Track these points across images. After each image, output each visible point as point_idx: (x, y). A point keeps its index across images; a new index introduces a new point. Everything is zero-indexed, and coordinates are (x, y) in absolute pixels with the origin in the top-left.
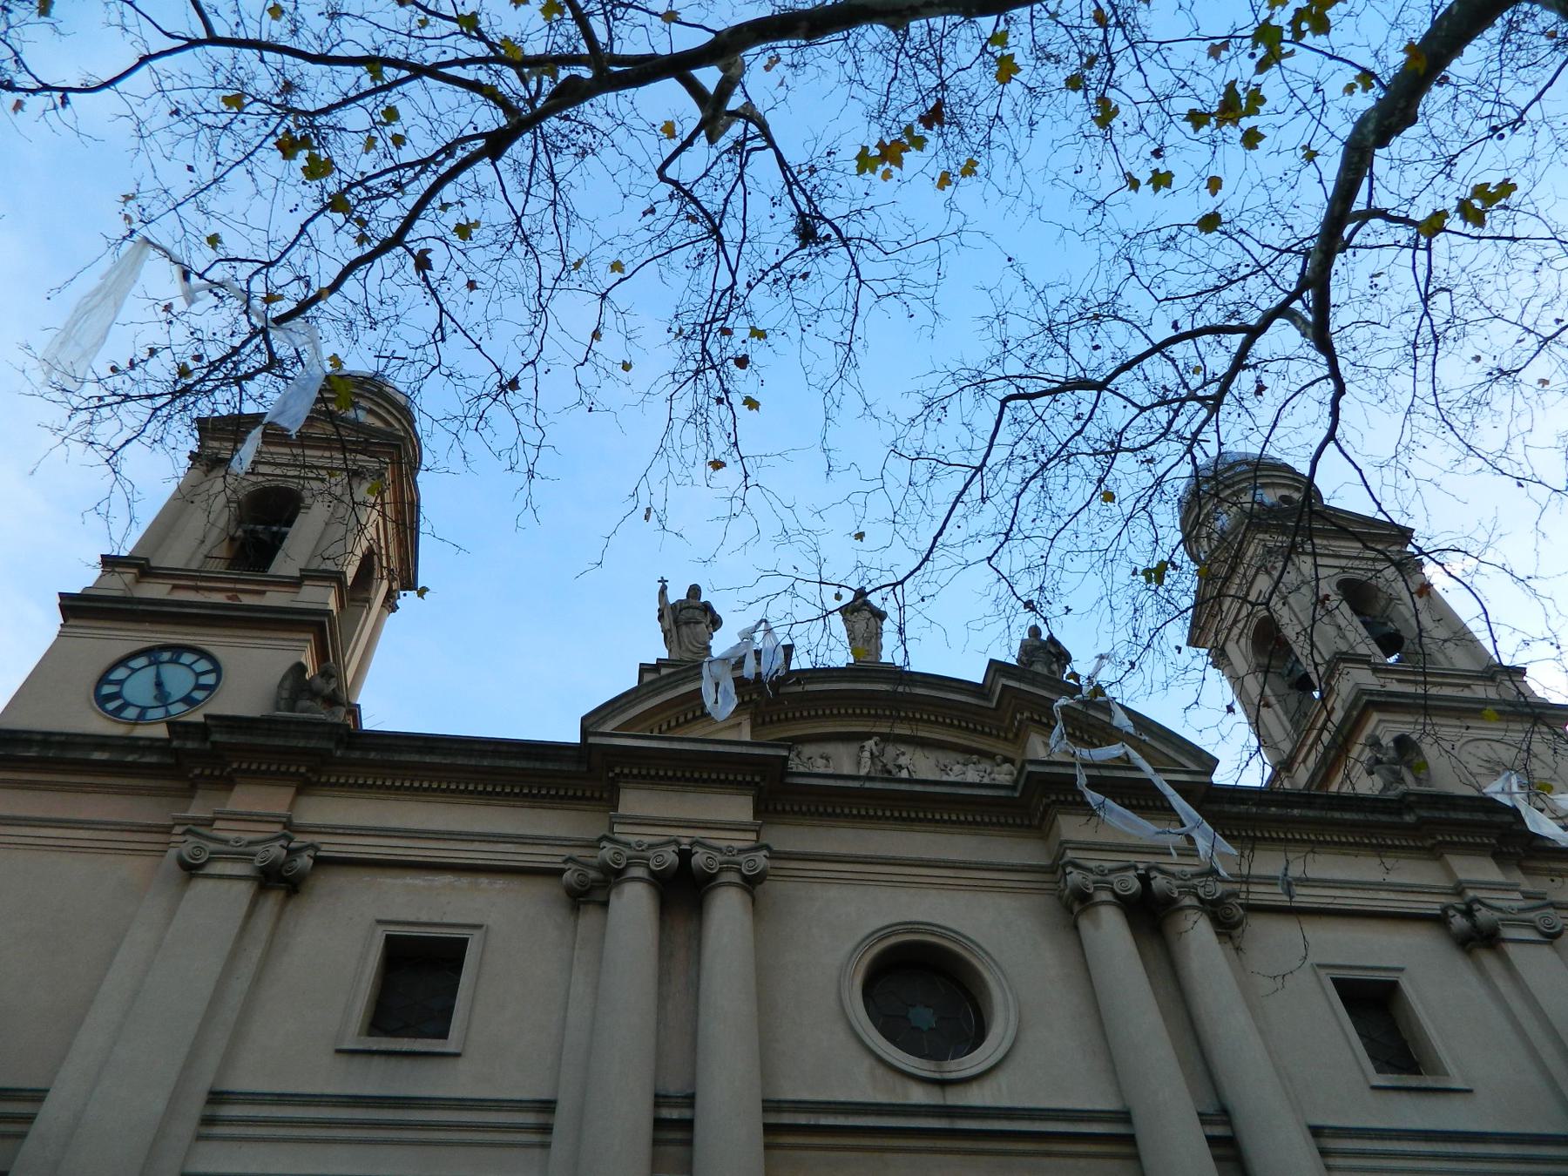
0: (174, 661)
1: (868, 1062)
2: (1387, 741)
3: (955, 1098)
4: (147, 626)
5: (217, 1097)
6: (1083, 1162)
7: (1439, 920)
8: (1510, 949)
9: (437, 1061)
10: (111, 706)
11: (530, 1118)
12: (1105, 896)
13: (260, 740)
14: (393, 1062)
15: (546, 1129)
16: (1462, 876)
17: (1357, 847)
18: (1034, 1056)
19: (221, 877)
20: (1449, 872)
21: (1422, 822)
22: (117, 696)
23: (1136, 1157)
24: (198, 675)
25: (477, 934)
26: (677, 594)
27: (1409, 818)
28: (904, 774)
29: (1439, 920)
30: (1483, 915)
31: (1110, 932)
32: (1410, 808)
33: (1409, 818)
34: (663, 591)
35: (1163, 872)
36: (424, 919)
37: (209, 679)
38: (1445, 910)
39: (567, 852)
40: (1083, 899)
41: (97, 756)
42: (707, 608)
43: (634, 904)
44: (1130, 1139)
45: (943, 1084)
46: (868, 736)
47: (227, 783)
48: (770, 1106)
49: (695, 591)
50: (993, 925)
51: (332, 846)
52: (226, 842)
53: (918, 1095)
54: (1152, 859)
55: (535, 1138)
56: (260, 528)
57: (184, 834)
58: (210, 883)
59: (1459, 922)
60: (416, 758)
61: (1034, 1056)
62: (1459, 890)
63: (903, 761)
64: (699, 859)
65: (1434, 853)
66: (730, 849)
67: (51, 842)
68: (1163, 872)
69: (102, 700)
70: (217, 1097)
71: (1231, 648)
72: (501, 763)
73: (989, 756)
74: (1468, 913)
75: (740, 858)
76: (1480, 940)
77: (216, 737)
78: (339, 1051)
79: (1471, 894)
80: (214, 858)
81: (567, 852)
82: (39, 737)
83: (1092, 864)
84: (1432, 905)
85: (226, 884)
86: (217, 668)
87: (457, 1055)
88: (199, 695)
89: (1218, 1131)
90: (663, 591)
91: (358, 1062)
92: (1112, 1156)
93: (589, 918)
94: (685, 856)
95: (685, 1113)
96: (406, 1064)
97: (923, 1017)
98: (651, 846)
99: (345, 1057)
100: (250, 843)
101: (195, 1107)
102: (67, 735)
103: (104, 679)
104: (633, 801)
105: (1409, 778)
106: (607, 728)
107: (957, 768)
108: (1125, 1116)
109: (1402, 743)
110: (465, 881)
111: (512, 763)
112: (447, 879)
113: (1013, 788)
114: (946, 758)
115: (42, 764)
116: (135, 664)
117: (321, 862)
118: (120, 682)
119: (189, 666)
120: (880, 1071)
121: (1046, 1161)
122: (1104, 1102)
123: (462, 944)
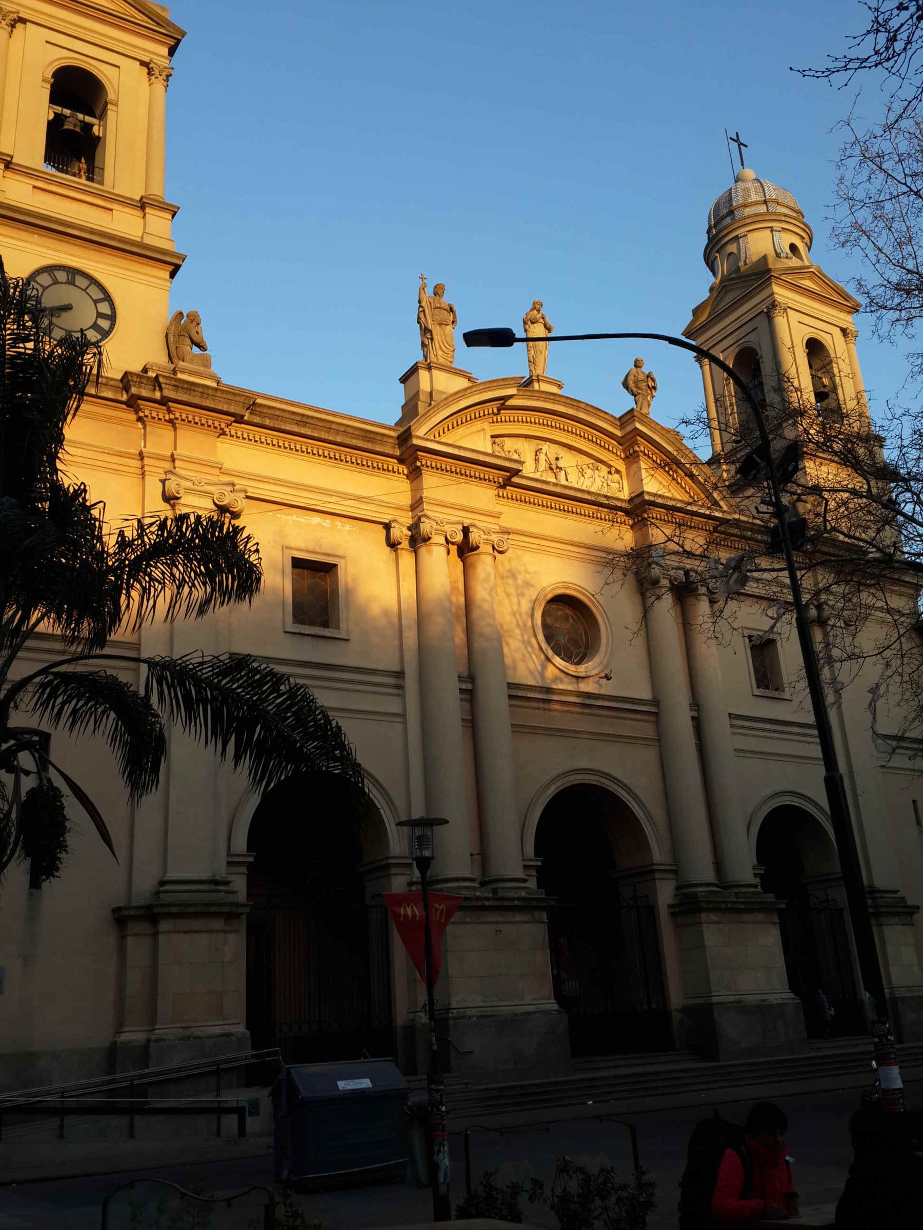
0: (71, 283)
6: (634, 723)
11: (391, 681)
14: (315, 641)
15: (401, 687)
24: (96, 302)
25: (342, 561)
37: (104, 308)
55: (395, 691)
56: (67, 112)
64: (474, 537)
78: (285, 632)
86: (108, 298)
87: (348, 640)
88: (104, 324)
89: (695, 714)
91: (297, 637)
94: (466, 531)
95: (470, 687)
96: (322, 643)
107: (589, 472)
108: (656, 702)
119: (85, 290)
122: (646, 695)
123: (335, 566)
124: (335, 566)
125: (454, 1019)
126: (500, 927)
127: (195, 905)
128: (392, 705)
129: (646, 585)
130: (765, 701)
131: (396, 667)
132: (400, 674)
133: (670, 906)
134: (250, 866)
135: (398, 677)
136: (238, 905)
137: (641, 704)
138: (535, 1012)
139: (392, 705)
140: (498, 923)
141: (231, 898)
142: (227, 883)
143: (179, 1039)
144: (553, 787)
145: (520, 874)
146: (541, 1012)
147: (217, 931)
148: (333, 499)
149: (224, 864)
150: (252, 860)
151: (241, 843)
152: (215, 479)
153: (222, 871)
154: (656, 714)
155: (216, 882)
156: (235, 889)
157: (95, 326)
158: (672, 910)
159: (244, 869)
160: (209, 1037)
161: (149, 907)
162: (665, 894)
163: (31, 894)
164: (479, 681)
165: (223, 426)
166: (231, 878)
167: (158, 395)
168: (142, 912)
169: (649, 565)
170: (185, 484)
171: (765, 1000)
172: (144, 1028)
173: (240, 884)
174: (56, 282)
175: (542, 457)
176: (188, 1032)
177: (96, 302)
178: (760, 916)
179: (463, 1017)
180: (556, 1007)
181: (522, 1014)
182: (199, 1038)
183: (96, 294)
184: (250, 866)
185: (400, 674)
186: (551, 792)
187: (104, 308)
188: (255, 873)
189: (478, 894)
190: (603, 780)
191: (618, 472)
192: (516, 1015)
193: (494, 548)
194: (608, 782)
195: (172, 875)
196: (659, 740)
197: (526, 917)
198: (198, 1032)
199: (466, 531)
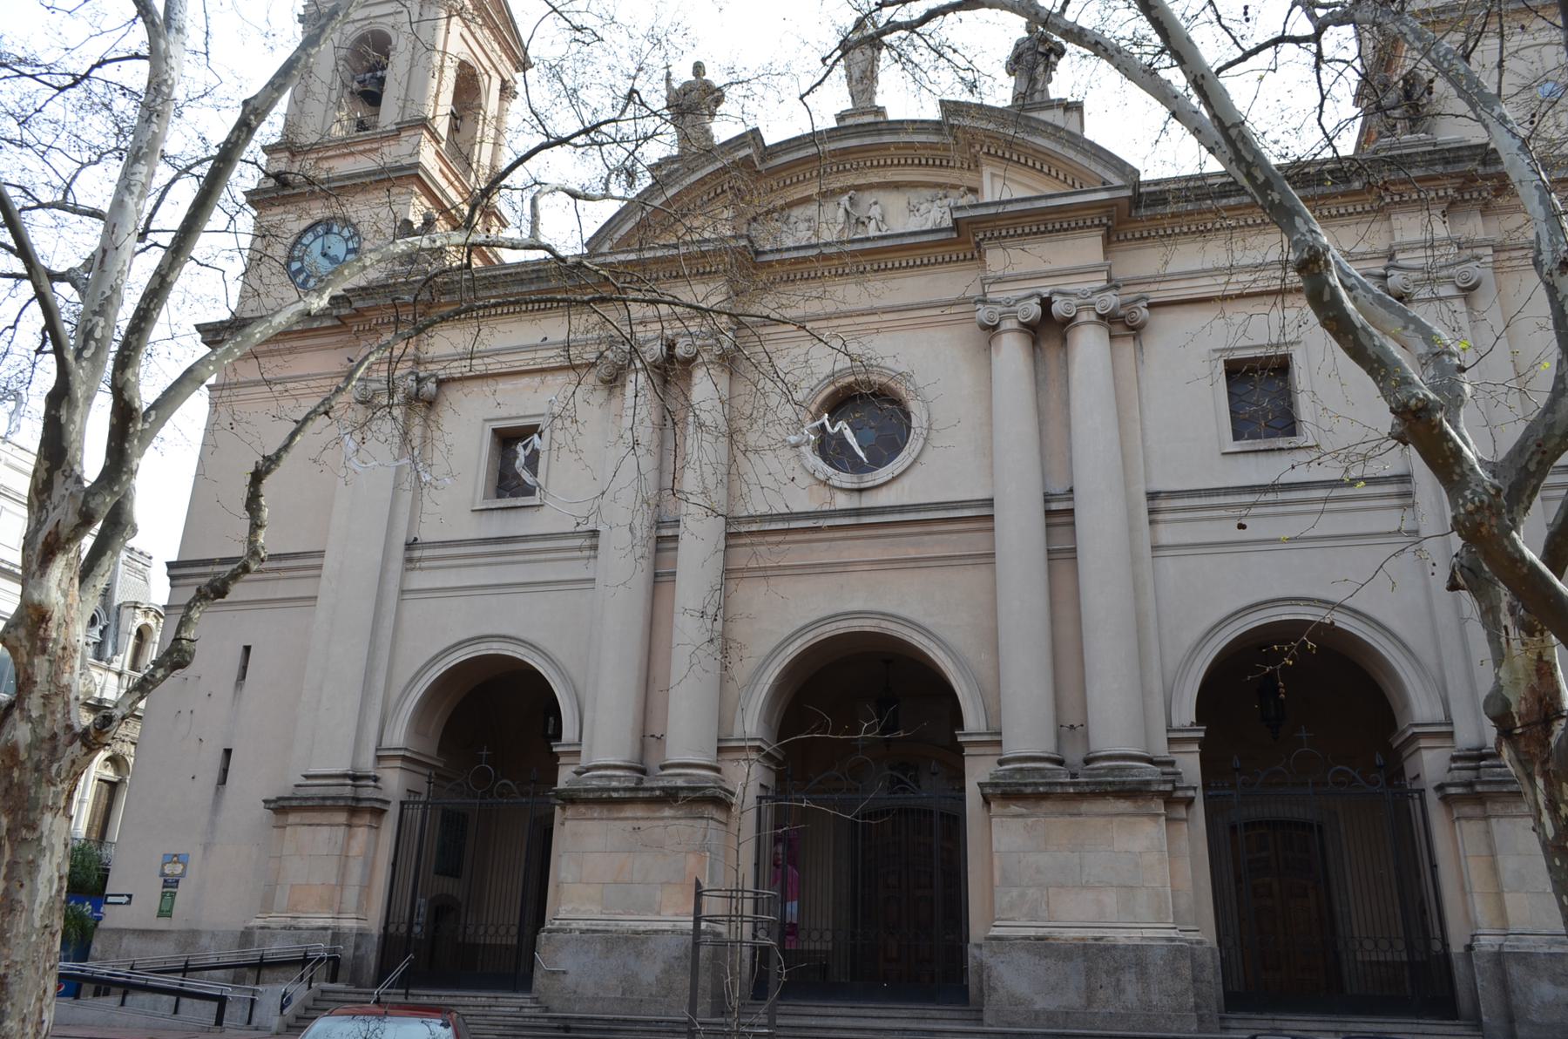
3: (868, 501)
5: (411, 545)
6: (955, 537)
22: (300, 271)
35: (1064, 294)
53: (842, 501)
55: (586, 553)
68: (1064, 294)
116: (305, 241)
117: (440, 383)
121: (927, 538)
125: (550, 931)
126: (641, 824)
127: (312, 798)
128: (577, 570)
130: (1262, 458)
137: (962, 508)
171: (1101, 938)
176: (293, 922)
179: (563, 931)
181: (645, 932)
190: (884, 624)
194: (892, 626)
198: (302, 923)
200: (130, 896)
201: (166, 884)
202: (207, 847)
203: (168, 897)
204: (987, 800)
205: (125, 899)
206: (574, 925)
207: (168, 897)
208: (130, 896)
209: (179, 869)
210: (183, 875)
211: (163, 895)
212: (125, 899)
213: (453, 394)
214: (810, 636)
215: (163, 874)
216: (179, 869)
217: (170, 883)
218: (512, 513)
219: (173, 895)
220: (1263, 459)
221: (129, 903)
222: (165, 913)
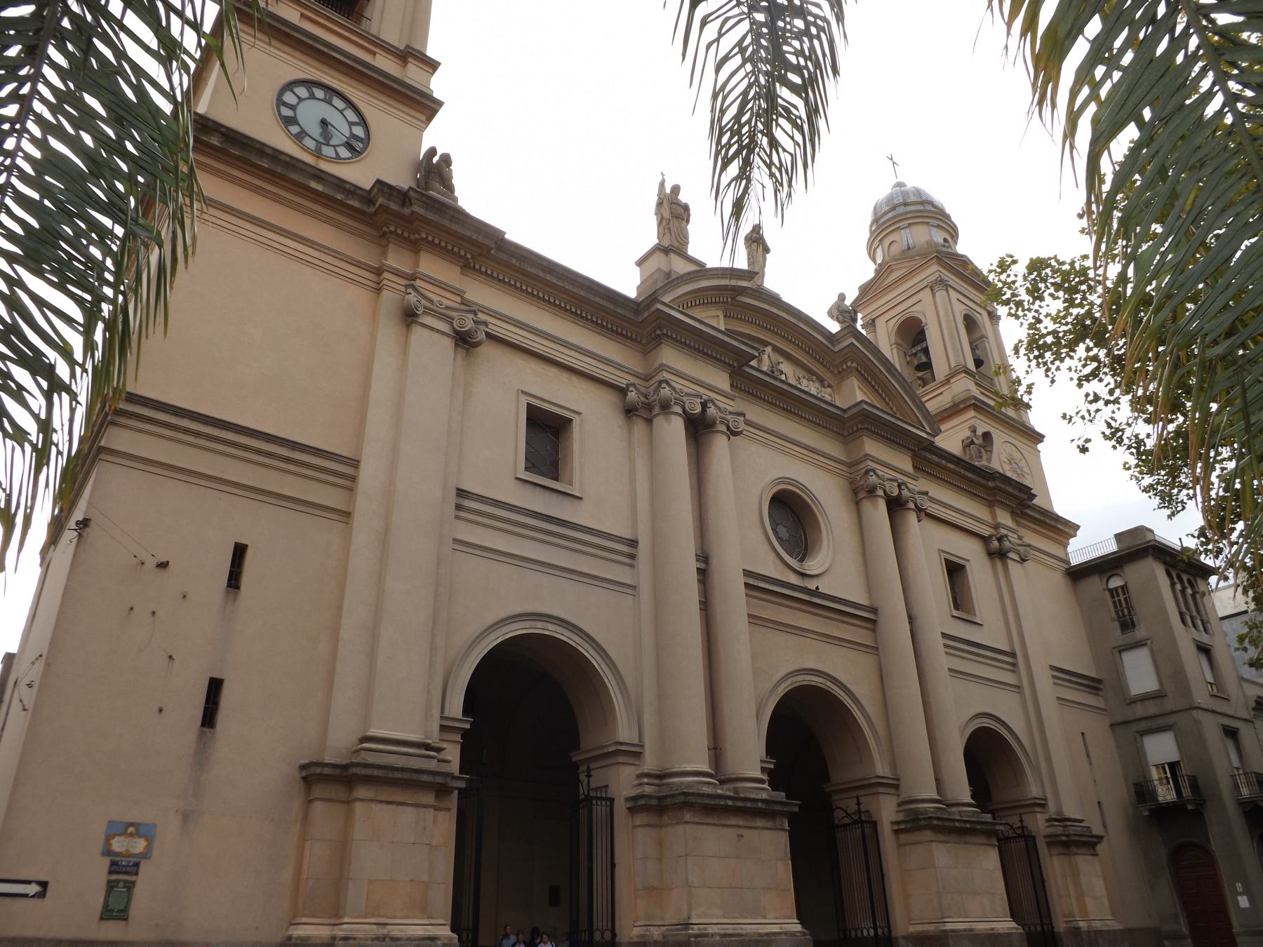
1: (773, 555)
2: (980, 432)
3: (812, 585)
4: (298, 54)
7: (985, 540)
8: (1009, 562)
9: (570, 499)
10: (295, 129)
11: (625, 549)
12: (880, 492)
13: (447, 223)
14: (547, 494)
15: (632, 557)
16: (1000, 520)
17: (974, 495)
18: (835, 567)
19: (432, 329)
20: (994, 516)
21: (995, 488)
23: (874, 631)
24: (351, 124)
26: (668, 191)
27: (991, 484)
28: (783, 377)
29: (985, 540)
30: (1007, 544)
31: (879, 512)
32: (994, 479)
33: (991, 484)
34: (662, 184)
36: (546, 397)
37: (359, 131)
38: (990, 536)
39: (633, 380)
40: (871, 492)
41: (313, 185)
42: (686, 208)
43: (673, 430)
44: (874, 622)
45: (803, 575)
46: (766, 344)
47: (415, 246)
48: (747, 573)
49: (676, 189)
50: (825, 491)
51: (498, 328)
52: (431, 301)
53: (793, 579)
54: (906, 479)
57: (406, 286)
58: (426, 332)
59: (996, 543)
60: (541, 274)
61: (835, 567)
62: (996, 527)
63: (782, 367)
65: (991, 504)
66: (725, 411)
67: (291, 251)
69: (289, 121)
70: (461, 493)
71: (880, 324)
72: (591, 297)
73: (821, 381)
74: (1000, 539)
75: (729, 417)
76: (998, 554)
77: (417, 209)
78: (518, 479)
79: (1003, 531)
80: (428, 312)
81: (633, 380)
82: (270, 152)
83: (880, 473)
84: (987, 531)
85: (437, 336)
86: (363, 122)
87: (580, 499)
88: (358, 146)
90: (662, 184)
91: (529, 488)
92: (866, 628)
93: (639, 428)
97: (782, 531)
98: (687, 394)
99: (520, 483)
100: (447, 308)
101: (452, 499)
102: (292, 158)
103: (280, 102)
104: (669, 356)
105: (985, 456)
106: (667, 299)
108: (874, 610)
109: (987, 436)
110: (565, 376)
111: (598, 300)
112: (554, 371)
113: (845, 411)
114: (801, 373)
115: (270, 176)
118: (292, 107)
119: (341, 112)
120: (778, 562)
122: (863, 601)
123: (570, 421)
124: (570, 421)
128: (623, 574)
129: (862, 494)
131: (627, 534)
132: (633, 543)
133: (893, 823)
134: (465, 734)
135: (629, 545)
136: (453, 777)
138: (780, 933)
139: (623, 574)
140: (739, 827)
141: (444, 768)
142: (439, 750)
143: (373, 939)
144: (783, 686)
145: (757, 774)
146: (785, 933)
147: (426, 806)
148: (572, 353)
149: (436, 728)
150: (468, 726)
151: (456, 707)
152: (456, 306)
153: (434, 738)
154: (874, 622)
155: (427, 747)
156: (449, 758)
157: (349, 146)
158: (896, 827)
159: (458, 738)
160: (409, 939)
161: (345, 767)
162: (887, 811)
163: (201, 735)
164: (714, 562)
165: (469, 256)
166: (444, 745)
167: (406, 211)
168: (337, 772)
169: (867, 472)
170: (424, 302)
172: (327, 921)
173: (453, 754)
174: (312, 97)
175: (765, 357)
176: (382, 931)
177: (351, 124)
178: (982, 840)
179: (706, 935)
180: (799, 928)
181: (767, 934)
182: (398, 939)
183: (352, 116)
184: (465, 734)
185: (633, 543)
186: (781, 691)
187: (359, 131)
188: (470, 743)
189: (719, 791)
190: (829, 684)
191: (829, 386)
192: (760, 935)
193: (728, 428)
195: (375, 732)
196: (877, 649)
197: (769, 824)
198: (395, 932)
199: (704, 406)
200: (44, 885)
201: (115, 868)
202: (186, 817)
203: (121, 888)
204: (896, 832)
205: (33, 889)
206: (711, 930)
207: (121, 888)
208: (44, 885)
209: (139, 846)
210: (146, 855)
211: (111, 886)
212: (33, 889)
213: (489, 351)
214: (789, 682)
215: (108, 852)
216: (139, 846)
217: (123, 871)
218: (554, 496)
219: (130, 886)
220: (962, 625)
221: (42, 895)
222: (114, 911)
